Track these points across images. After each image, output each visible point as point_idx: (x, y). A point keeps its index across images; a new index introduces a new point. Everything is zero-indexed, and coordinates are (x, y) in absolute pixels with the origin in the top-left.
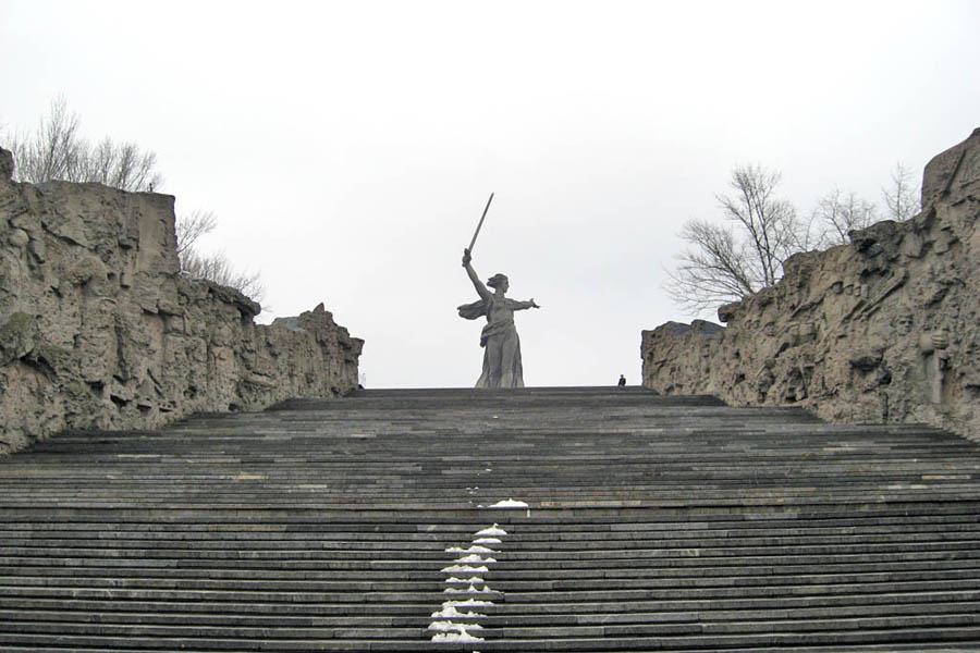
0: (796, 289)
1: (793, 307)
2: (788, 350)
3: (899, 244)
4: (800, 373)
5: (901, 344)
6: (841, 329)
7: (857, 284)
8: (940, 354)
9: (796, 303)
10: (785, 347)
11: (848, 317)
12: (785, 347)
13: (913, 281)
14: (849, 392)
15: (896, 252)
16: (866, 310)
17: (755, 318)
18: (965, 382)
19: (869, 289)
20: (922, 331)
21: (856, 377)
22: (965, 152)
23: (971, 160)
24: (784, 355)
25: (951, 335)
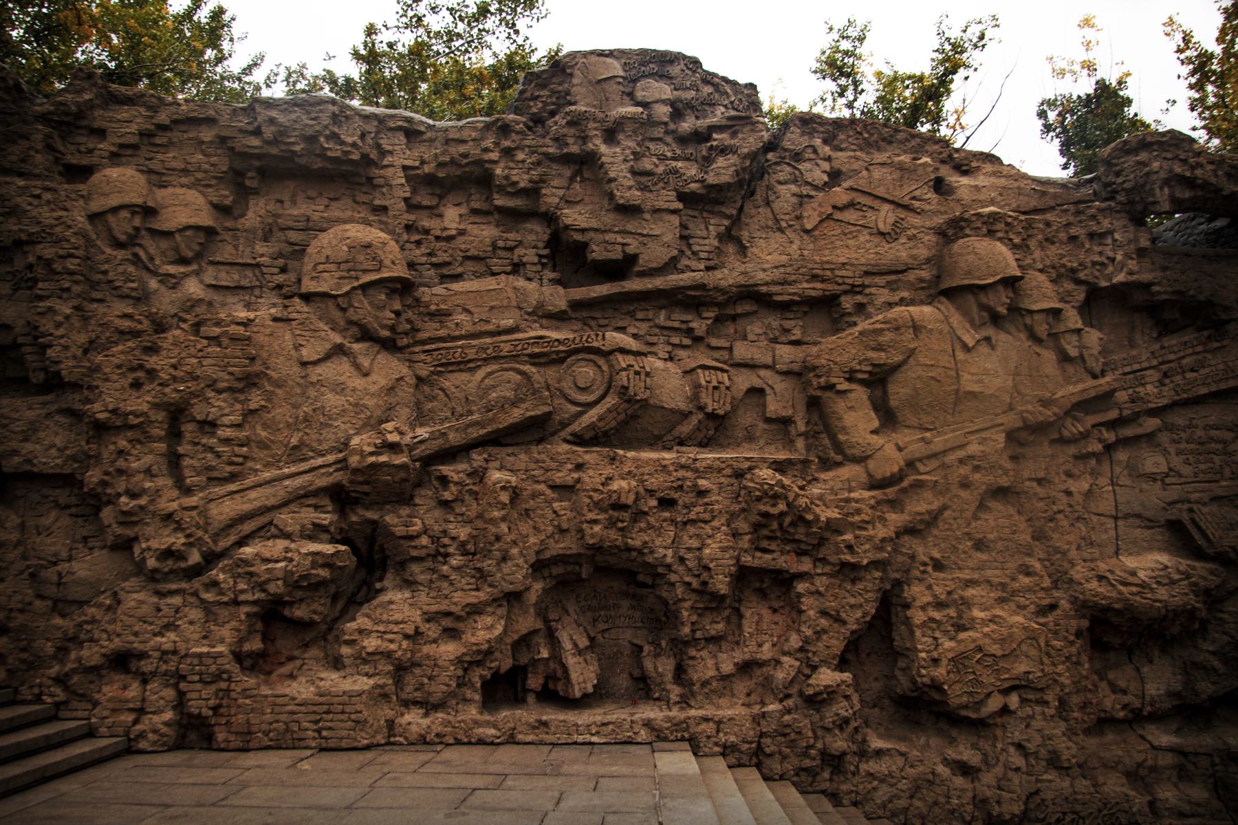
0: (666, 198)
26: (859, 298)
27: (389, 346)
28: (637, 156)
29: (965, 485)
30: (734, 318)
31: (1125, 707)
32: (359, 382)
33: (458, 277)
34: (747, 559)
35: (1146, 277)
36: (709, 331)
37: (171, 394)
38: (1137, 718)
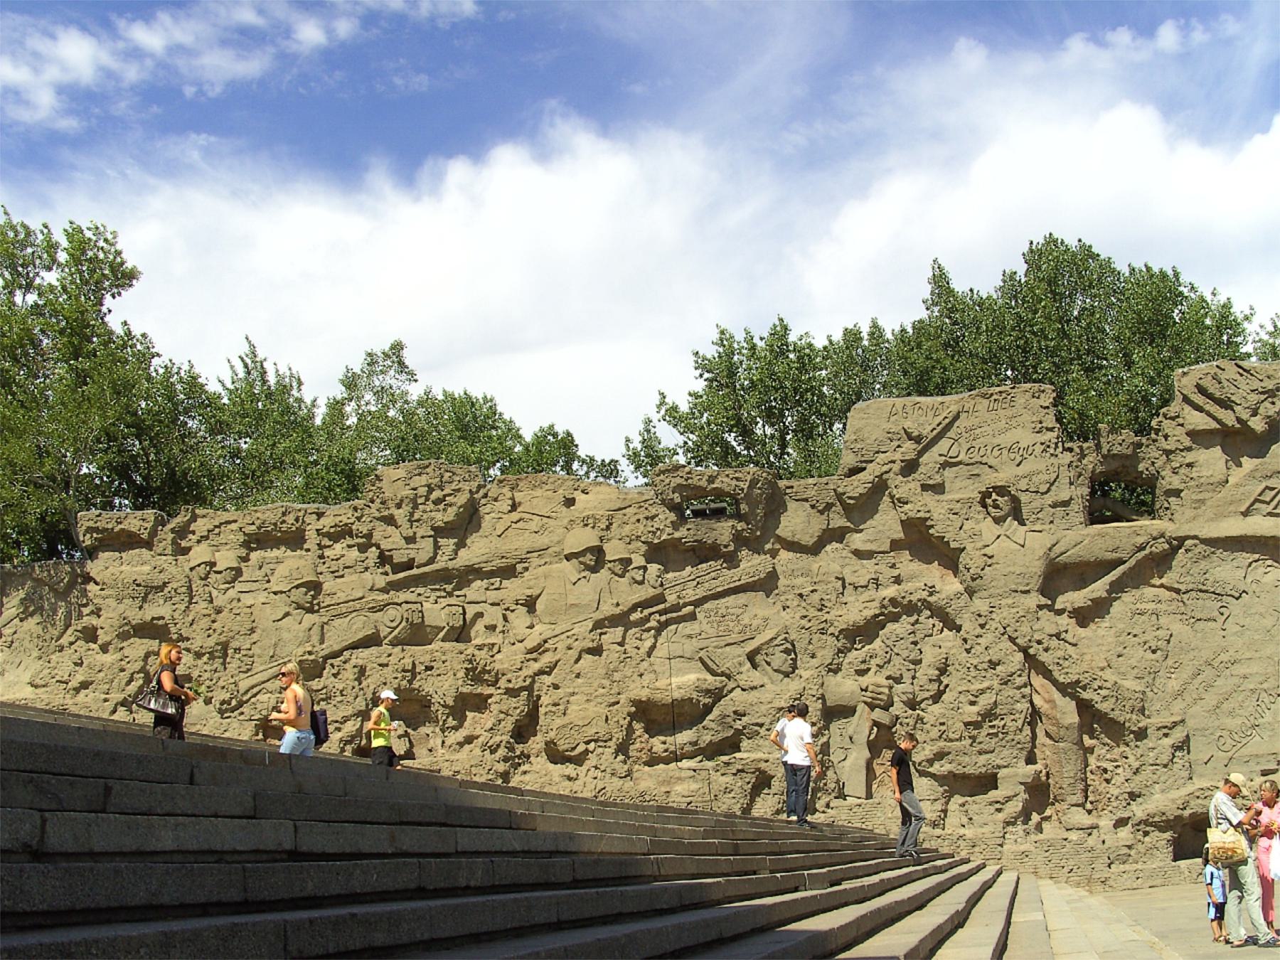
0: (424, 530)
7: (638, 560)
10: (372, 641)
12: (372, 641)
17: (226, 559)
24: (362, 656)
26: (526, 565)
27: (310, 610)
28: (412, 514)
31: (666, 751)
32: (297, 627)
33: (342, 576)
36: (454, 590)
37: (223, 639)
38: (675, 757)
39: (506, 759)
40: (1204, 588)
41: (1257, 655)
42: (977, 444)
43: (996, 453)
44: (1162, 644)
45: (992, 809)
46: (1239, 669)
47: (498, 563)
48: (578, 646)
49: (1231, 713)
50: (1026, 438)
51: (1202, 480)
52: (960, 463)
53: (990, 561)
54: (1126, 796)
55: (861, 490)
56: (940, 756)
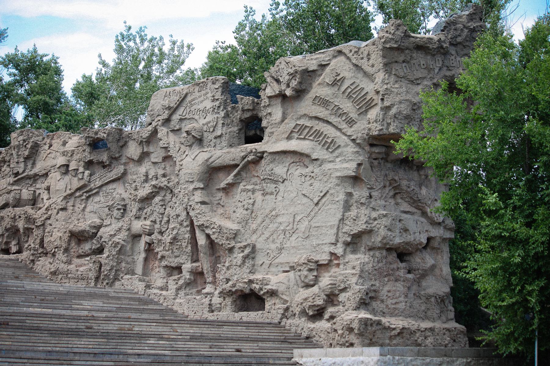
1: (17, 174)
2: (7, 209)
3: (122, 147)
4: (18, 230)
5: (116, 225)
6: (64, 202)
7: (81, 169)
8: (145, 239)
9: (21, 171)
11: (71, 195)
13: (129, 177)
14: (66, 255)
15: (119, 152)
16: (86, 192)
18: (164, 263)
19: (91, 175)
20: (133, 219)
21: (73, 244)
22: (186, 95)
23: (190, 102)
25: (157, 226)
29: (55, 208)
30: (37, 179)
34: (25, 226)
35: (91, 158)
39: (33, 255)
40: (270, 178)
41: (286, 212)
42: (192, 109)
43: (198, 113)
44: (250, 206)
45: (175, 282)
46: (280, 219)
47: (44, 172)
48: (57, 207)
49: (273, 241)
50: (208, 104)
51: (272, 122)
52: (186, 118)
53: (181, 168)
54: (225, 280)
55: (147, 135)
56: (163, 257)
